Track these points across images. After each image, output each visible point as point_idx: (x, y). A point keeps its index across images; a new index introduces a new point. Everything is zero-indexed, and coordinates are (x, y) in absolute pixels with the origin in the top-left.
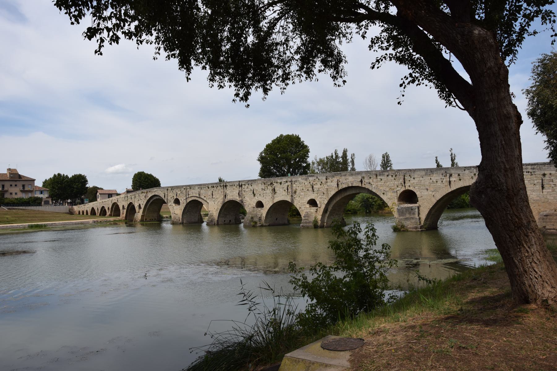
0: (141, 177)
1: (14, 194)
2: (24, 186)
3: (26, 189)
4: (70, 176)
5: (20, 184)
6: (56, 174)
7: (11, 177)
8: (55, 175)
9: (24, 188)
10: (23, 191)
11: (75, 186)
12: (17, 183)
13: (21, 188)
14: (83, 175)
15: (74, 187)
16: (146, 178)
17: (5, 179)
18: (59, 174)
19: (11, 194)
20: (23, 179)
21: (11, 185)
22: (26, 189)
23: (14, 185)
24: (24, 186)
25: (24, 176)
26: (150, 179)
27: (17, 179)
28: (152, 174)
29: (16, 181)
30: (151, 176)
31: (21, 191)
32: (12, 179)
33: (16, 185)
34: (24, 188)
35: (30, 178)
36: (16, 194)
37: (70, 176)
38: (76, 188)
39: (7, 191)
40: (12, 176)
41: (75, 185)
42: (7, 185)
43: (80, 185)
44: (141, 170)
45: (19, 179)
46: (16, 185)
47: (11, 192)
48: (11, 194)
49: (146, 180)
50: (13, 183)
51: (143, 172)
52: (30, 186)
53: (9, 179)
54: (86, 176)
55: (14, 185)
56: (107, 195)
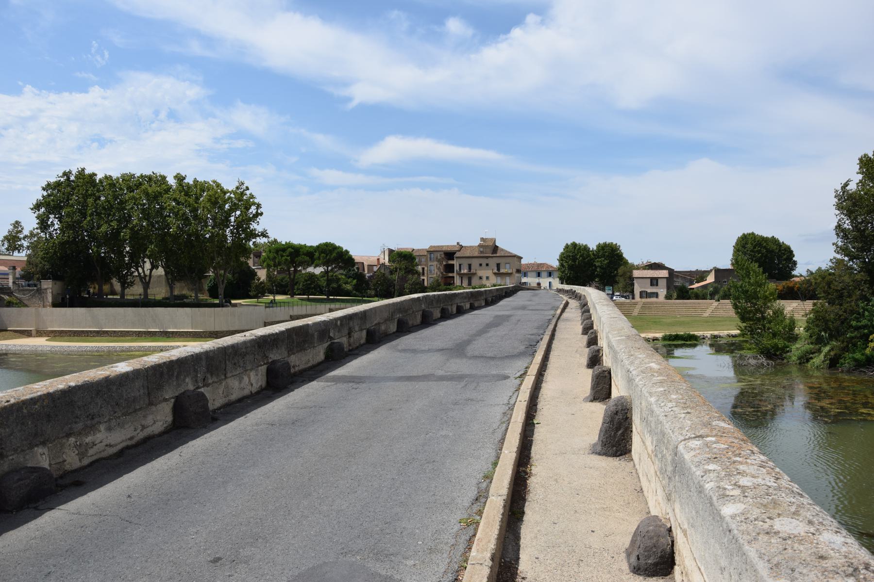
0: (746, 243)
1: (484, 279)
2: (498, 266)
3: (502, 271)
4: (593, 246)
5: (493, 262)
6: (569, 244)
7: (481, 252)
8: (567, 246)
9: (498, 269)
10: (498, 274)
11: (597, 264)
12: (489, 261)
13: (496, 271)
14: (614, 243)
15: (596, 267)
16: (756, 245)
17: (471, 256)
18: (574, 245)
19: (481, 278)
20: (498, 255)
21: (481, 265)
22: (502, 271)
23: (484, 265)
24: (498, 266)
25: (502, 250)
26: (765, 247)
27: (486, 255)
28: (776, 236)
29: (487, 257)
30: (774, 240)
31: (495, 274)
32: (482, 255)
33: (487, 265)
34: (498, 269)
35: (509, 253)
36: (487, 278)
37: (593, 246)
38: (600, 267)
39: (475, 274)
40: (482, 249)
41: (598, 261)
42: (475, 263)
43: (606, 262)
44: (747, 231)
45: (492, 254)
46: (487, 265)
47: (481, 275)
48: (481, 278)
49: (757, 249)
50: (484, 262)
51: (753, 234)
52: (508, 266)
53: (476, 254)
54: (619, 246)
55: (484, 265)
56: (649, 280)
